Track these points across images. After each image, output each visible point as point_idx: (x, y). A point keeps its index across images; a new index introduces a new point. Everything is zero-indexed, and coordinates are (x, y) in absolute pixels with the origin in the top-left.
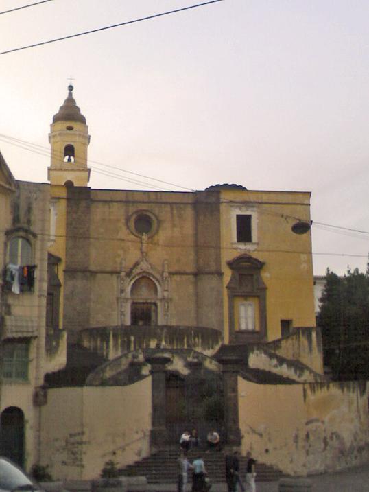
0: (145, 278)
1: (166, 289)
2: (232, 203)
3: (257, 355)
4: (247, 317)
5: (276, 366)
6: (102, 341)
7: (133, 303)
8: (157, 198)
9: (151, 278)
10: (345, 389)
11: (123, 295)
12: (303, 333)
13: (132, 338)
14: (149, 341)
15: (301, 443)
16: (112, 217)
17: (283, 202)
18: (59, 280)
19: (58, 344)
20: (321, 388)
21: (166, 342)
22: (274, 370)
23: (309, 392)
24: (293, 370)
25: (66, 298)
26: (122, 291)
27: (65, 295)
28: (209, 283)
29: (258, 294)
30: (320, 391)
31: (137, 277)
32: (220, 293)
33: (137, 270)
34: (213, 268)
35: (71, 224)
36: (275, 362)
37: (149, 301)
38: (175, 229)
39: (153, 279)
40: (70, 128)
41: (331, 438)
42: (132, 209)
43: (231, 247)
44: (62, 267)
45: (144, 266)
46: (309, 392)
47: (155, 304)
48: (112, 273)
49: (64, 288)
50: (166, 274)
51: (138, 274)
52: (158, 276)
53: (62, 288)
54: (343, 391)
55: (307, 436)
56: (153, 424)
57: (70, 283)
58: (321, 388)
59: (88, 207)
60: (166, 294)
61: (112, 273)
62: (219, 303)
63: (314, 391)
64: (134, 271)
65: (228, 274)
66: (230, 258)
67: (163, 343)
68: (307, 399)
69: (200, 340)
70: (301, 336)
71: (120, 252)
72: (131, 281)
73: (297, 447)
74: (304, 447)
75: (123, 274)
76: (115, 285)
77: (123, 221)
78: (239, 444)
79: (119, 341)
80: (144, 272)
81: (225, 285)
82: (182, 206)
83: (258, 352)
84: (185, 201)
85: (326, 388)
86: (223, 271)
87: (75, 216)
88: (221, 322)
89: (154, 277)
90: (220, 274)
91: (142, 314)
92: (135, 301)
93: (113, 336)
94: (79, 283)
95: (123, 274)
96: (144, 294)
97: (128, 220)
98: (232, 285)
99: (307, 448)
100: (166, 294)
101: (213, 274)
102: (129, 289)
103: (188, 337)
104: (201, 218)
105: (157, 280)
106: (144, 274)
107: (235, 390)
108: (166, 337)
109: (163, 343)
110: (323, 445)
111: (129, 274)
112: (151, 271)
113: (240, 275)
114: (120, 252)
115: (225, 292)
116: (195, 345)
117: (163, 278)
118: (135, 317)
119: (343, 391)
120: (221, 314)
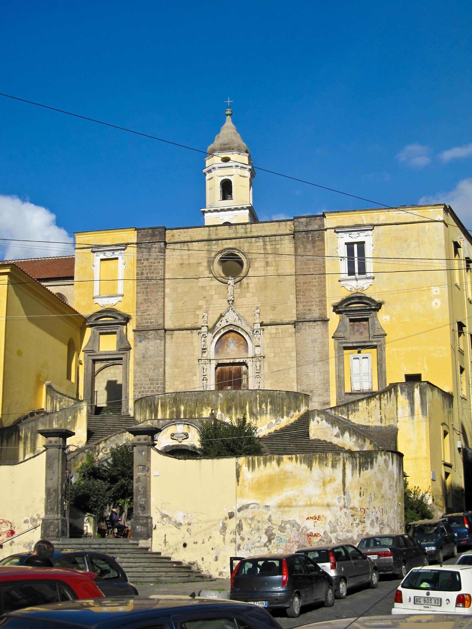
0: (232, 331)
1: (257, 344)
2: (338, 230)
3: (318, 422)
4: (361, 372)
5: (337, 436)
6: (151, 413)
7: (219, 365)
8: (246, 233)
9: (240, 331)
10: (315, 465)
11: (205, 355)
12: (402, 391)
13: (182, 408)
14: (202, 410)
15: (229, 537)
16: (192, 261)
17: (408, 221)
18: (128, 342)
19: (75, 418)
20: (265, 464)
21: (222, 411)
22: (335, 441)
23: (244, 468)
24: (354, 439)
25: (137, 364)
26: (204, 350)
27: (135, 359)
28: (313, 332)
29: (375, 343)
30: (262, 466)
31: (223, 332)
32: (325, 345)
33: (224, 323)
34: (316, 314)
35: (142, 274)
36: (336, 430)
37: (237, 361)
38: (268, 268)
39: (242, 334)
40: (226, 160)
41: (282, 529)
42: (216, 247)
43: (340, 285)
44: (131, 326)
45: (231, 317)
46: (244, 468)
48: (191, 329)
49: (134, 352)
50: (258, 326)
52: (248, 330)
53: (132, 351)
54: (310, 466)
55: (240, 527)
56: (46, 511)
57: (142, 345)
58: (265, 464)
59: (163, 251)
61: (191, 329)
62: (325, 359)
63: (253, 468)
64: (218, 325)
65: (335, 320)
66: (338, 300)
67: (219, 412)
68: (240, 479)
69: (269, 407)
70: (399, 393)
71: (202, 303)
72: (214, 337)
73: (224, 539)
74: (234, 541)
75: (204, 329)
77: (206, 264)
78: (149, 536)
79: (168, 412)
81: (331, 334)
82: (278, 238)
83: (319, 419)
84: (280, 232)
85: (274, 463)
86: (328, 317)
87: (146, 263)
88: (326, 383)
90: (325, 321)
91: (230, 377)
92: (220, 362)
93: (162, 405)
94: (152, 345)
95: (204, 329)
96: (232, 353)
97: (210, 263)
98: (341, 335)
99: (239, 541)
100: (258, 351)
101: (315, 321)
102: (212, 348)
103: (250, 403)
104: (300, 251)
106: (231, 329)
107: (146, 468)
108: (222, 405)
109: (219, 412)
110: (265, 539)
111: (210, 330)
112: (238, 323)
113: (351, 320)
114: (202, 303)
115: (332, 342)
116: (262, 413)
118: (220, 385)
119: (310, 466)
120: (327, 372)
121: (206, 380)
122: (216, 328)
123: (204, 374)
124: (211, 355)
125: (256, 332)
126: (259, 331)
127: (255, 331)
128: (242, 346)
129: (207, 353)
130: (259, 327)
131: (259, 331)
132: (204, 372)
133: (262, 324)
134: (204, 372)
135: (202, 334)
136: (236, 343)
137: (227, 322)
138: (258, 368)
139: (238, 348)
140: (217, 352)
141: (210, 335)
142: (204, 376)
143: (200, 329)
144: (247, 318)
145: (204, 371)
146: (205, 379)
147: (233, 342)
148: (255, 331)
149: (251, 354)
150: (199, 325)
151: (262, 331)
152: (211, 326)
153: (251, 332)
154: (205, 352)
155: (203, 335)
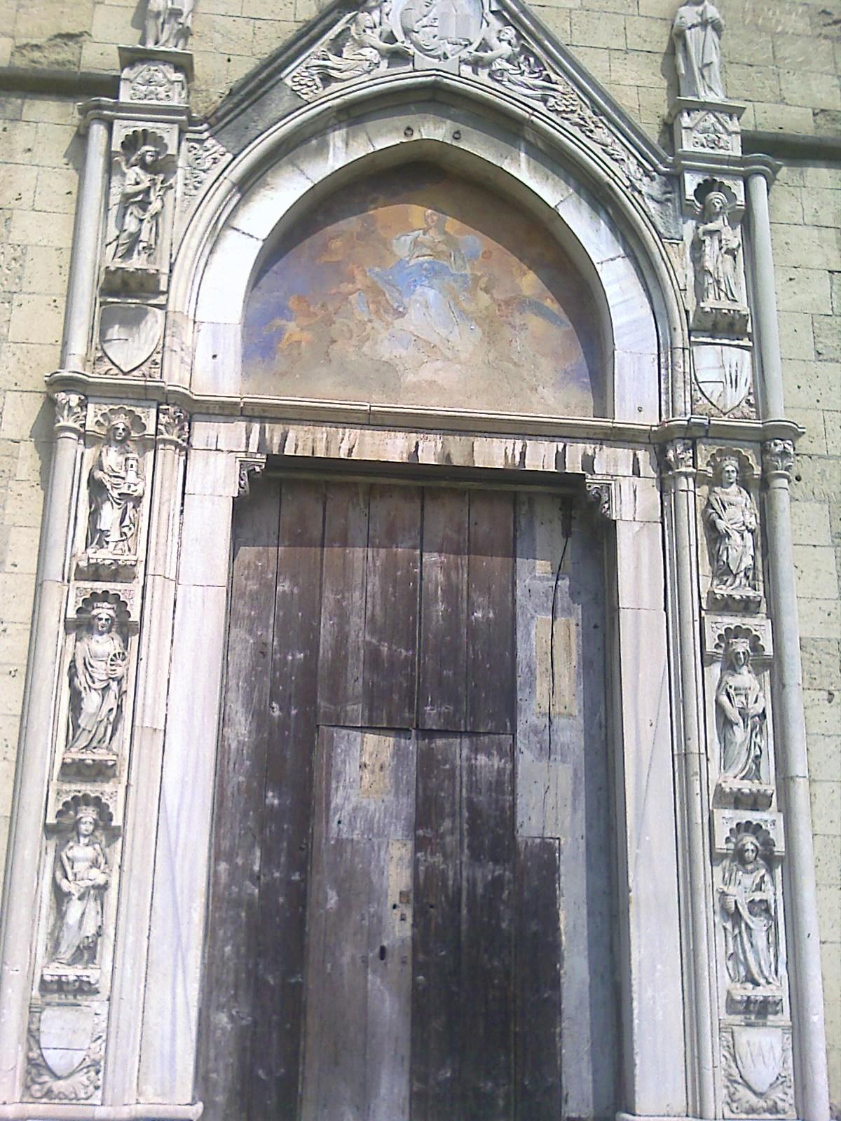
9: (522, 169)
11: (129, 351)
26: (128, 293)
31: (341, 152)
33: (361, 70)
37: (492, 453)
39: (550, 191)
47: (580, 515)
51: (354, 113)
60: (719, 371)
72: (248, 185)
76: (41, 230)
80: (435, 97)
89: (556, 158)
92: (301, 441)
105: (599, 196)
112: (518, 90)
117: (674, 180)
121: (126, 628)
122: (278, 102)
123: (104, 555)
124: (203, 362)
125: (702, 191)
126: (738, 188)
127: (691, 182)
128: (536, 323)
129: (154, 323)
130: (735, 148)
131: (738, 188)
132: (96, 535)
133: (751, 142)
134: (96, 535)
135: (122, 131)
136: (472, 284)
137: (397, 57)
138: (741, 551)
139: (491, 337)
140: (260, 341)
141: (210, 164)
142: (95, 572)
143: (110, 86)
144: (595, 64)
145: (109, 516)
146: (104, 611)
147: (434, 272)
148: (691, 182)
149: (637, 401)
150: (98, 56)
151: (760, 183)
152: (220, 71)
153: (650, 187)
154: (133, 320)
155: (131, 144)
